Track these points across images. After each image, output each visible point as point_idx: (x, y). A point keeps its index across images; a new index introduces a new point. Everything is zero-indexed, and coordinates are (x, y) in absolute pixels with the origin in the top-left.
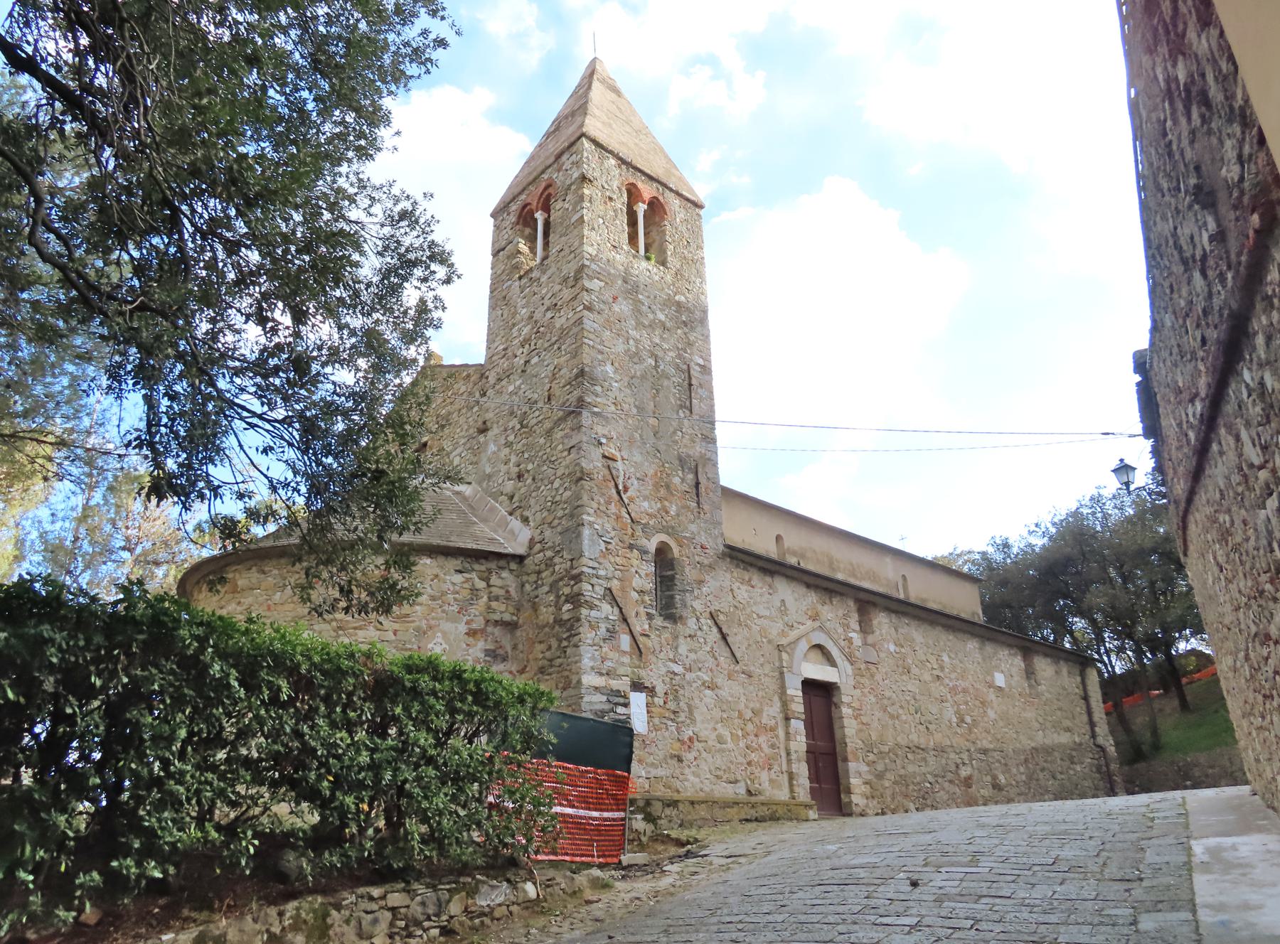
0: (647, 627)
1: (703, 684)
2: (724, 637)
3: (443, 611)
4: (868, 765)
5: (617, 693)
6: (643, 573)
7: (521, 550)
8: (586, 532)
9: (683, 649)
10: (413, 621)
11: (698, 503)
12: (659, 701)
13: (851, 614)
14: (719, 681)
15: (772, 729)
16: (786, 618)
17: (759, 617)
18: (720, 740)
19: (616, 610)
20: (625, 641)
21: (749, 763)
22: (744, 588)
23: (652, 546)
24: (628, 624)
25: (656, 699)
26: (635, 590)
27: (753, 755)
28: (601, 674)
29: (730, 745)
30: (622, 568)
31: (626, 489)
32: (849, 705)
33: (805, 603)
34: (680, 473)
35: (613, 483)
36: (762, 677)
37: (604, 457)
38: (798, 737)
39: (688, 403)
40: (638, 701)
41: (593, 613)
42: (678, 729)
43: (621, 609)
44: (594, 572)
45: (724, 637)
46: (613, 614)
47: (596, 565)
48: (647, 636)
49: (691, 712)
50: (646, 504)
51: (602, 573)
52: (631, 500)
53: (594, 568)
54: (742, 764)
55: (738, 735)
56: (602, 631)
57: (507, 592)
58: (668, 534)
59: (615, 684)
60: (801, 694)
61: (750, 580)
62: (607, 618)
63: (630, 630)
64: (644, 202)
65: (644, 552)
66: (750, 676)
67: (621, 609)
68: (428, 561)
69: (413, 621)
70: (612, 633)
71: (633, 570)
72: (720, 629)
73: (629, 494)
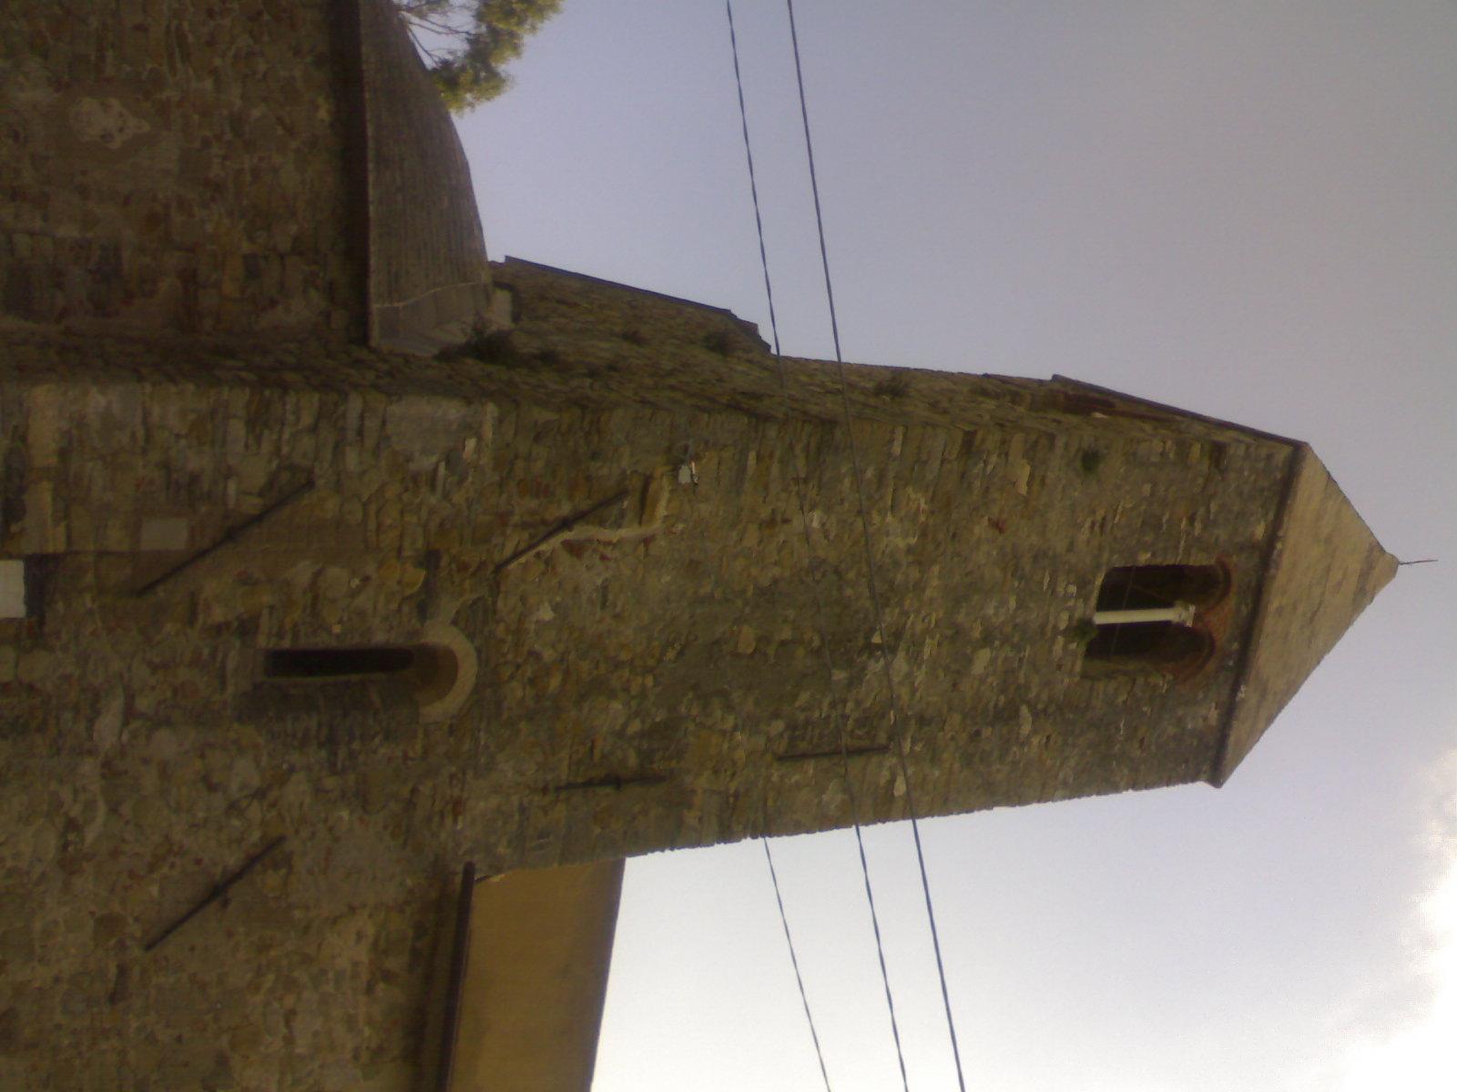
0: (218, 614)
1: (72, 825)
2: (217, 892)
3: (206, 143)
6: (363, 601)
7: (373, 343)
8: (452, 410)
9: (166, 744)
10: (173, 68)
11: (570, 786)
17: (290, 1015)
19: (252, 505)
20: (168, 535)
22: (363, 954)
23: (442, 634)
24: (217, 545)
26: (318, 574)
28: (64, 454)
30: (372, 525)
31: (575, 549)
34: (635, 726)
35: (585, 505)
37: (647, 480)
39: (803, 746)
41: (237, 428)
43: (258, 518)
44: (351, 435)
45: (217, 892)
46: (241, 495)
47: (370, 442)
48: (192, 619)
50: (546, 614)
51: (352, 460)
52: (549, 562)
53: (360, 432)
56: (199, 461)
57: (273, 303)
58: (478, 688)
59: (42, 498)
61: (388, 976)
62: (229, 473)
63: (203, 554)
64: (1197, 617)
66: (113, 998)
67: (258, 518)
68: (324, 114)
69: (173, 68)
71: (370, 569)
72: (239, 875)
73: (565, 559)
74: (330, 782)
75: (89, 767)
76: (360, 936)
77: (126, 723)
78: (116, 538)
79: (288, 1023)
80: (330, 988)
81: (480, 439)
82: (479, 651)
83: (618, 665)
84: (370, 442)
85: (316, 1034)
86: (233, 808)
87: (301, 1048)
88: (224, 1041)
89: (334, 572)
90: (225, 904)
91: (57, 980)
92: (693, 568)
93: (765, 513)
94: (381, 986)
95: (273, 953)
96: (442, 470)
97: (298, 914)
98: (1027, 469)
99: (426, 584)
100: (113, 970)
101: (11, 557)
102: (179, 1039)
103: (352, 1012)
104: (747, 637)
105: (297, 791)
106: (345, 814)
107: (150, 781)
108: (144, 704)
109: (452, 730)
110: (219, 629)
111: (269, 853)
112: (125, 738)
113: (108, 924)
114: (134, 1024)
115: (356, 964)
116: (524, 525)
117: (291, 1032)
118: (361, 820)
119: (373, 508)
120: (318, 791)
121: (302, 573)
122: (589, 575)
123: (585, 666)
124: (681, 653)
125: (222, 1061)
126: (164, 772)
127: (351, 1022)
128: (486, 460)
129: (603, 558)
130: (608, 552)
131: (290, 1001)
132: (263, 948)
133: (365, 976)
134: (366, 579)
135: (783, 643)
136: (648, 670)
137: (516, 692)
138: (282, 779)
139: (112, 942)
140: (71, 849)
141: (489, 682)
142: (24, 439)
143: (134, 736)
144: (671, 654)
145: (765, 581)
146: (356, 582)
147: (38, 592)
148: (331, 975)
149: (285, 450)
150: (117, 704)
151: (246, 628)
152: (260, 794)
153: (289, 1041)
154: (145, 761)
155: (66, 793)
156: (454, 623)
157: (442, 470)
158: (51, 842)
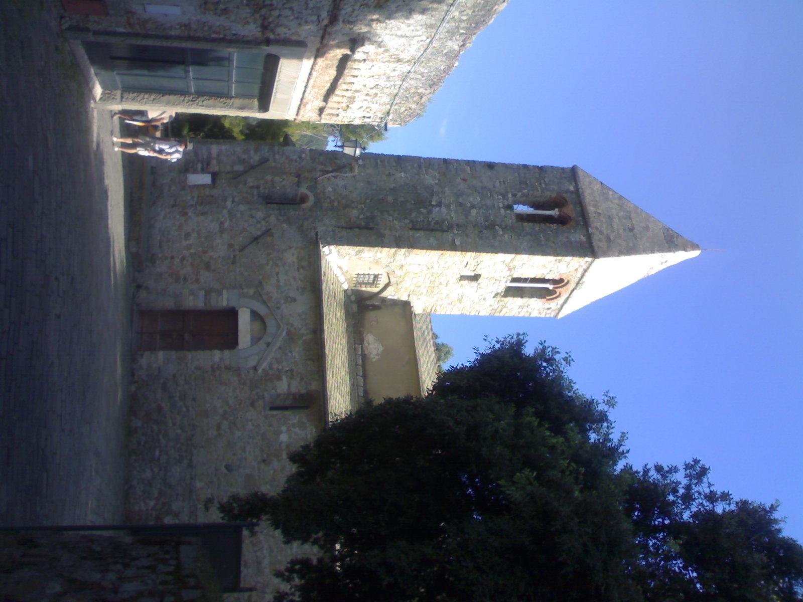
0: (251, 184)
4: (174, 376)
5: (208, 164)
9: (242, 208)
12: (207, 191)
14: (225, 236)
15: (197, 280)
16: (282, 301)
17: (277, 274)
18: (188, 235)
20: (239, 168)
21: (172, 258)
22: (294, 259)
23: (303, 190)
29: (185, 243)
30: (283, 167)
31: (335, 177)
32: (221, 359)
34: (362, 216)
38: (191, 298)
40: (206, 179)
41: (252, 152)
42: (192, 205)
43: (257, 166)
45: (256, 239)
49: (203, 214)
50: (330, 189)
51: (277, 157)
56: (245, 156)
59: (214, 162)
60: (225, 304)
61: (303, 267)
65: (298, 184)
66: (233, 263)
70: (243, 161)
71: (284, 177)
74: (280, 218)
75: (225, 211)
76: (293, 255)
78: (228, 168)
81: (305, 154)
82: (314, 195)
83: (353, 202)
85: (285, 280)
86: (258, 222)
88: (261, 277)
89: (277, 179)
90: (258, 243)
91: (219, 257)
92: (369, 183)
93: (387, 172)
94: (301, 270)
95: (271, 256)
96: (298, 159)
98: (469, 168)
100: (232, 256)
101: (208, 173)
104: (390, 199)
105: (272, 219)
106: (285, 225)
107: (239, 215)
108: (236, 199)
109: (310, 210)
110: (252, 187)
111: (267, 232)
113: (230, 246)
116: (320, 171)
120: (278, 220)
121: (269, 178)
122: (341, 183)
125: (261, 283)
127: (294, 278)
128: (308, 158)
131: (277, 269)
132: (269, 254)
134: (284, 179)
135: (402, 202)
136: (361, 204)
137: (325, 205)
138: (269, 216)
141: (318, 202)
144: (368, 201)
145: (392, 187)
146: (281, 180)
147: (214, 180)
148: (287, 264)
150: (231, 200)
151: (258, 187)
152: (264, 219)
153: (278, 281)
154: (237, 211)
155: (220, 216)
156: (306, 189)
158: (217, 226)
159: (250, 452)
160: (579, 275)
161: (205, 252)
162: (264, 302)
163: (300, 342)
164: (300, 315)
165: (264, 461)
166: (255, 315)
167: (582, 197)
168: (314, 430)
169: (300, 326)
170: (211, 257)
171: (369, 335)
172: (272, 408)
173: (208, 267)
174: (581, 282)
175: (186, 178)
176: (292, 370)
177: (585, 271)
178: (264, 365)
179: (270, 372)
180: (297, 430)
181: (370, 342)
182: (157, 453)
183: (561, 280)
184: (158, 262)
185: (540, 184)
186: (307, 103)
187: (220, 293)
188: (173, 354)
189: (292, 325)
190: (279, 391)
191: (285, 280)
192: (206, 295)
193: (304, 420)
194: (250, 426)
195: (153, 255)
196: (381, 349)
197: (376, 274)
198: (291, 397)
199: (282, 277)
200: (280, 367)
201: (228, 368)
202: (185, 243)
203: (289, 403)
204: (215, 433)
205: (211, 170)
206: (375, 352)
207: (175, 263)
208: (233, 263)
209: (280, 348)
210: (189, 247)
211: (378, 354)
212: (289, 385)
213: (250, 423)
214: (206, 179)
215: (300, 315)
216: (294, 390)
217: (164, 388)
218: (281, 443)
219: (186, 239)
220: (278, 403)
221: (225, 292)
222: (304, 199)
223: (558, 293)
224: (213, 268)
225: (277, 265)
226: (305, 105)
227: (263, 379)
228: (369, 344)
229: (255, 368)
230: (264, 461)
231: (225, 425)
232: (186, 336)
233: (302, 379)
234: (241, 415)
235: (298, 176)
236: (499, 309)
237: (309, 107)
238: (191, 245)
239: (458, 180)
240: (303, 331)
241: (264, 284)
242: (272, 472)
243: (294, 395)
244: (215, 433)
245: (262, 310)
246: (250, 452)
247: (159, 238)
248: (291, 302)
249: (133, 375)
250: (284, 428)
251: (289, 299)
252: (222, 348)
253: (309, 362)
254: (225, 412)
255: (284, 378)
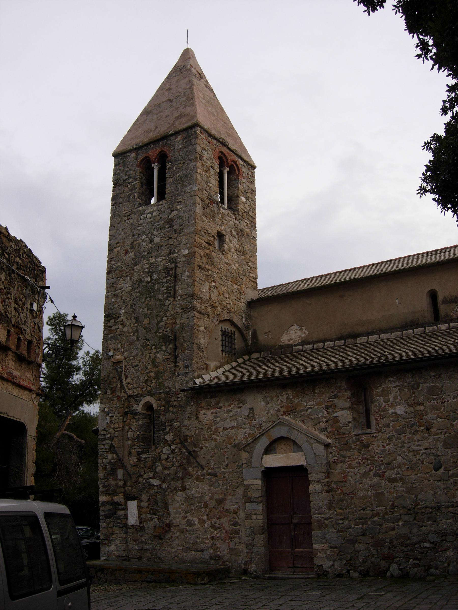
12: (144, 504)
13: (340, 395)
15: (235, 512)
16: (254, 422)
17: (225, 429)
18: (190, 523)
21: (213, 538)
23: (139, 408)
25: (142, 504)
27: (216, 532)
30: (118, 429)
33: (279, 402)
34: (164, 348)
36: (226, 475)
38: (254, 517)
40: (132, 506)
54: (207, 539)
55: (203, 520)
60: (259, 482)
61: (217, 403)
65: (135, 414)
66: (215, 475)
74: (168, 429)
77: (155, 478)
79: (228, 429)
80: (218, 419)
82: (144, 397)
83: (150, 357)
84: (105, 432)
87: (234, 424)
88: (229, 446)
91: (210, 490)
94: (220, 405)
96: (110, 415)
97: (197, 432)
98: (115, 250)
99: (131, 414)
100: (209, 477)
101: (126, 503)
102: (227, 458)
103: (226, 412)
105: (169, 437)
112: (158, 478)
113: (198, 479)
114: (223, 470)
115: (212, 413)
117: (230, 428)
118: (177, 419)
119: (116, 430)
123: (149, 367)
124: (148, 340)
125: (235, 446)
126: (164, 468)
127: (229, 411)
129: (128, 369)
130: (126, 368)
131: (221, 430)
132: (206, 440)
133: (217, 410)
138: (167, 441)
139: (202, 477)
140: (180, 489)
142: (107, 502)
143: (157, 476)
146: (130, 430)
148: (215, 420)
149: (107, 450)
150: (151, 481)
153: (232, 428)
154: (163, 473)
157: (110, 415)
159: (419, 445)
160: (215, 142)
161: (206, 505)
162: (256, 440)
163: (296, 401)
164: (267, 403)
165: (428, 429)
166: (269, 450)
167: (141, 144)
168: (391, 379)
169: (279, 402)
170: (211, 499)
171: (282, 340)
172: (369, 426)
173: (221, 501)
174: (221, 140)
175: (132, 526)
176: (327, 408)
177: (210, 135)
178: (323, 437)
179: (329, 430)
180: (391, 397)
181: (289, 338)
182: (427, 545)
183: (220, 158)
184: (218, 553)
185: (129, 183)
186: (10, 373)
187: (248, 488)
188: (316, 533)
189: (278, 410)
190: (350, 419)
191: (231, 421)
192: (251, 502)
193: (379, 390)
194: (391, 447)
195: (211, 558)
196: (296, 327)
197: (220, 333)
198: (356, 406)
199: (229, 423)
200: (324, 420)
201: (328, 475)
202: (197, 526)
203: (361, 409)
204: (400, 484)
205: (123, 501)
206: (299, 333)
207: (218, 535)
208: (215, 475)
209: (303, 421)
210: (202, 522)
211: (301, 330)
212: (343, 409)
213: (387, 447)
214: (132, 506)
215: (267, 403)
216: (347, 404)
217: (353, 542)
218: (406, 412)
219: (194, 525)
220: (362, 420)
221: (246, 483)
222: (148, 406)
223: (233, 163)
224: (221, 496)
225: (216, 430)
226: (14, 377)
227: (337, 437)
228: (291, 339)
229: (327, 446)
230: (428, 429)
231: (390, 474)
232: (295, 521)
233: (336, 396)
234: (378, 458)
235: (126, 414)
236: (250, 218)
237: (16, 373)
238: (199, 519)
239: (127, 258)
240: (284, 398)
241: (236, 442)
242: (439, 420)
243: (353, 403)
244: (400, 484)
245: (264, 442)
246: (419, 445)
247: (194, 552)
248: (253, 413)
249: (339, 576)
250: (391, 411)
251: (251, 415)
252: (308, 483)
253: (317, 390)
254: (376, 475)
255: (335, 415)
